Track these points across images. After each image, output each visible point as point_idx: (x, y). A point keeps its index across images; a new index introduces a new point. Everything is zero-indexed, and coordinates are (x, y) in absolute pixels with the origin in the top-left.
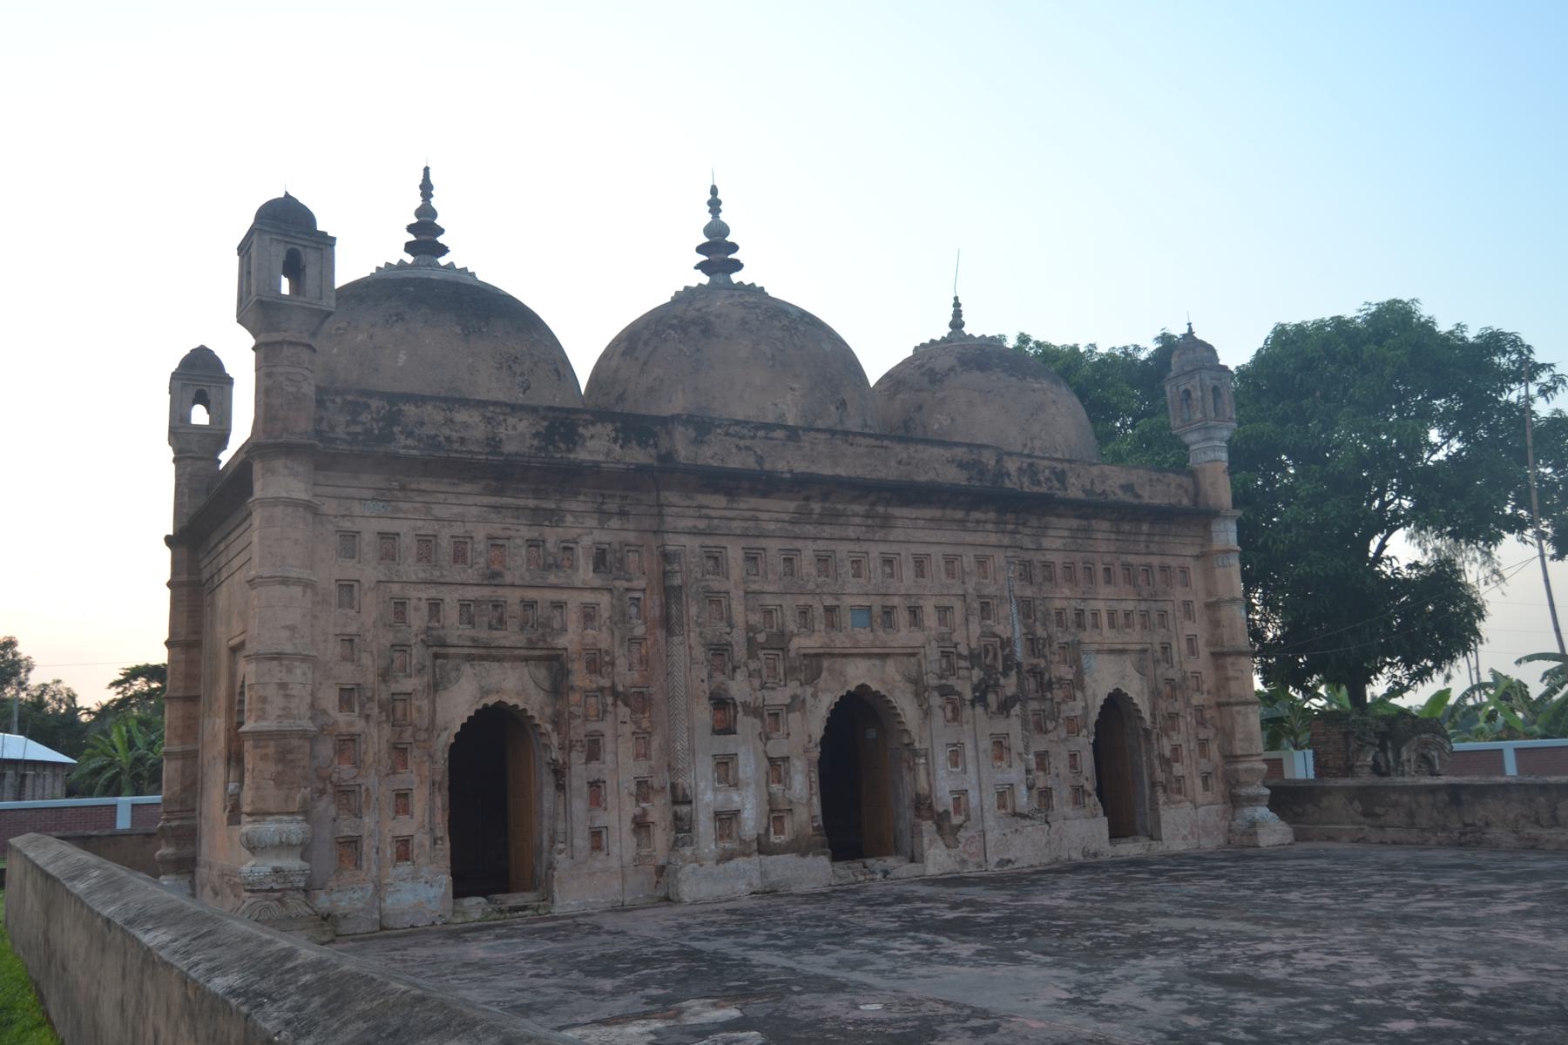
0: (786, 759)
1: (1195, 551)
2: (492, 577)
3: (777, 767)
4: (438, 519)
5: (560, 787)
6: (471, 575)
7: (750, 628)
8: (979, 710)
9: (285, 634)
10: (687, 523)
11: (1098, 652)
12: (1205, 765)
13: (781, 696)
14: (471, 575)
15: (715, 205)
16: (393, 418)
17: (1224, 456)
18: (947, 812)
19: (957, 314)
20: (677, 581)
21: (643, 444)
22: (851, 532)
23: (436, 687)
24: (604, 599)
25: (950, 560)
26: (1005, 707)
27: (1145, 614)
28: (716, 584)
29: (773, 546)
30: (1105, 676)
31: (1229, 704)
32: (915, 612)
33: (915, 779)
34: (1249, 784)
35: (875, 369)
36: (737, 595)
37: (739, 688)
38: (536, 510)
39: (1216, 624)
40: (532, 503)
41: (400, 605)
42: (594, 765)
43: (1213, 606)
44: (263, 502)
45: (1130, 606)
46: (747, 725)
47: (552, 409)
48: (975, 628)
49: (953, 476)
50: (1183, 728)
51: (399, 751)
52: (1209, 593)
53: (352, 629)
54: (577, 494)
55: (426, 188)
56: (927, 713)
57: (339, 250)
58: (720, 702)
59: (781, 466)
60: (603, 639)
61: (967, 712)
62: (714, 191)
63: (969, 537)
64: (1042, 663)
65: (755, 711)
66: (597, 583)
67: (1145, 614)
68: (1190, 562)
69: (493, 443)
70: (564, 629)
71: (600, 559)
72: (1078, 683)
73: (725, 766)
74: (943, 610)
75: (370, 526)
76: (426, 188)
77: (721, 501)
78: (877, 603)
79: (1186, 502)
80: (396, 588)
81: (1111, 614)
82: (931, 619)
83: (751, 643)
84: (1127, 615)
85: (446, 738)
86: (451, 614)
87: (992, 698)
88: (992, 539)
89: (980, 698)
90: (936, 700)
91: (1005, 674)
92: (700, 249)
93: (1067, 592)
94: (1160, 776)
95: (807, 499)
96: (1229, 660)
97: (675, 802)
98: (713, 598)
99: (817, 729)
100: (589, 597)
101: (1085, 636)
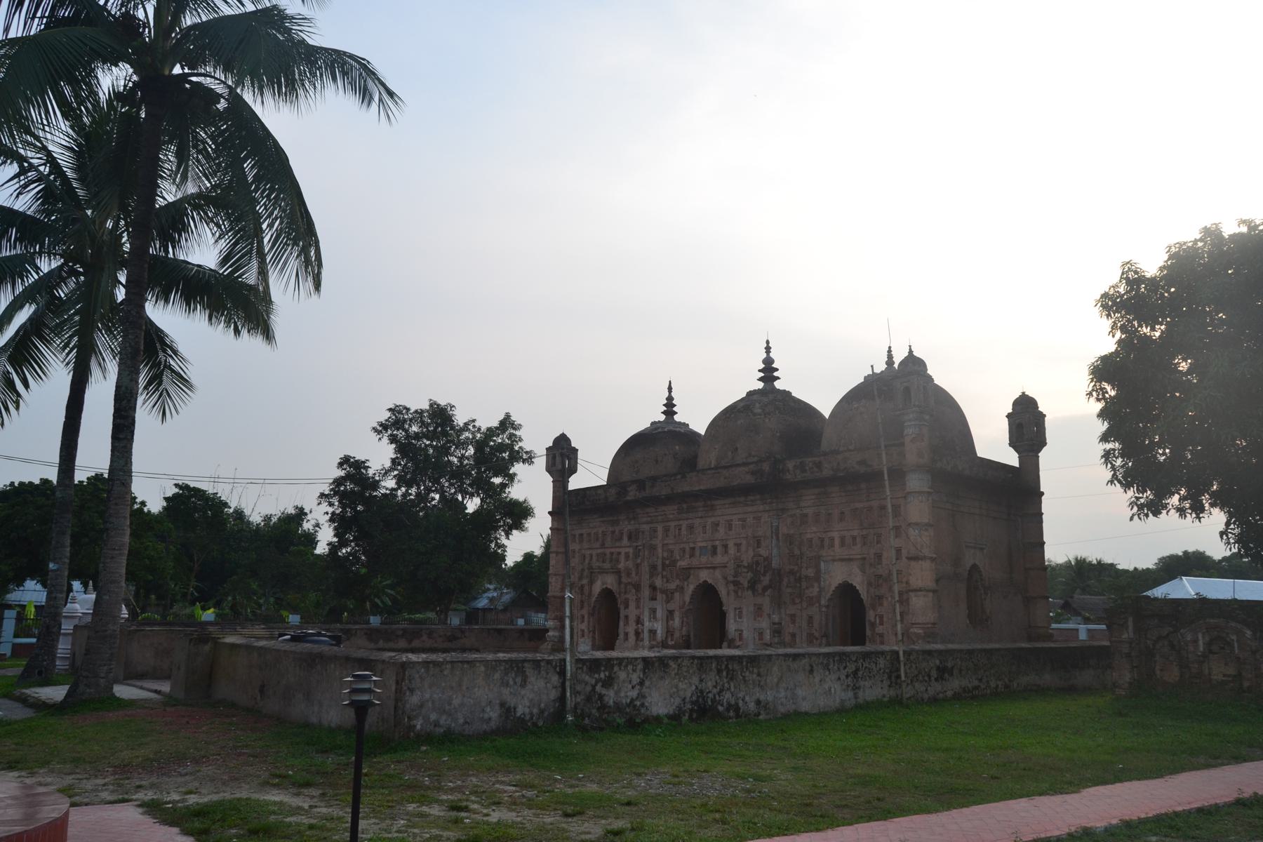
2: (603, 546)
7: (663, 558)
8: (750, 592)
11: (834, 561)
13: (672, 586)
14: (598, 545)
15: (768, 349)
18: (733, 640)
23: (591, 583)
26: (765, 589)
27: (864, 537)
29: (672, 524)
30: (836, 575)
32: (726, 546)
35: (826, 410)
37: (658, 582)
45: (855, 533)
46: (659, 596)
48: (751, 553)
49: (749, 479)
50: (885, 604)
51: (582, 602)
55: (670, 389)
58: (653, 588)
62: (768, 342)
63: (750, 509)
64: (796, 568)
65: (663, 592)
67: (864, 537)
71: (630, 538)
72: (817, 578)
74: (738, 545)
75: (577, 532)
76: (670, 389)
78: (710, 544)
81: (843, 539)
82: (732, 550)
83: (663, 564)
84: (854, 538)
86: (594, 558)
87: (759, 587)
88: (761, 508)
89: (752, 586)
90: (732, 587)
91: (764, 575)
93: (814, 529)
99: (687, 599)
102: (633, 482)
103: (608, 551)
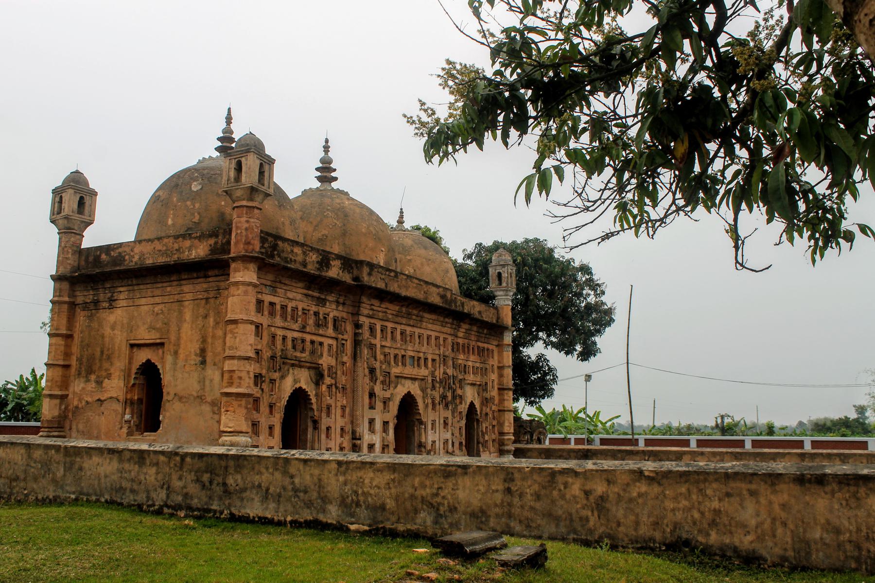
0: (387, 422)
1: (495, 343)
3: (386, 424)
4: (288, 298)
5: (316, 428)
6: (296, 326)
9: (250, 348)
10: (366, 312)
12: (494, 437)
14: (296, 326)
15: (326, 148)
16: (274, 247)
17: (510, 303)
19: (401, 217)
20: (360, 338)
21: (349, 272)
22: (411, 323)
23: (283, 377)
24: (334, 343)
25: (437, 338)
28: (373, 341)
29: (390, 325)
30: (470, 395)
31: (504, 411)
32: (426, 359)
33: (420, 435)
34: (507, 445)
36: (378, 346)
38: (318, 298)
39: (501, 376)
40: (316, 294)
41: (274, 337)
42: (328, 419)
43: (501, 368)
44: (237, 284)
45: (478, 365)
46: (379, 405)
47: (323, 251)
52: (499, 362)
53: (259, 347)
54: (332, 292)
56: (427, 406)
57: (276, 167)
58: (372, 395)
59: (392, 289)
60: (333, 362)
61: (438, 406)
62: (327, 141)
66: (333, 335)
68: (494, 348)
69: (304, 264)
70: (322, 355)
73: (372, 422)
74: (433, 360)
75: (268, 298)
77: (376, 302)
79: (494, 321)
80: (273, 329)
85: (284, 402)
92: (317, 169)
94: (481, 440)
95: (402, 306)
96: (506, 392)
97: (353, 439)
98: (372, 347)
100: (331, 341)
101: (467, 377)
102: (338, 257)
103: (308, 338)
